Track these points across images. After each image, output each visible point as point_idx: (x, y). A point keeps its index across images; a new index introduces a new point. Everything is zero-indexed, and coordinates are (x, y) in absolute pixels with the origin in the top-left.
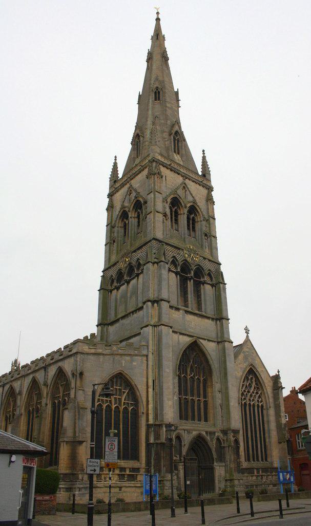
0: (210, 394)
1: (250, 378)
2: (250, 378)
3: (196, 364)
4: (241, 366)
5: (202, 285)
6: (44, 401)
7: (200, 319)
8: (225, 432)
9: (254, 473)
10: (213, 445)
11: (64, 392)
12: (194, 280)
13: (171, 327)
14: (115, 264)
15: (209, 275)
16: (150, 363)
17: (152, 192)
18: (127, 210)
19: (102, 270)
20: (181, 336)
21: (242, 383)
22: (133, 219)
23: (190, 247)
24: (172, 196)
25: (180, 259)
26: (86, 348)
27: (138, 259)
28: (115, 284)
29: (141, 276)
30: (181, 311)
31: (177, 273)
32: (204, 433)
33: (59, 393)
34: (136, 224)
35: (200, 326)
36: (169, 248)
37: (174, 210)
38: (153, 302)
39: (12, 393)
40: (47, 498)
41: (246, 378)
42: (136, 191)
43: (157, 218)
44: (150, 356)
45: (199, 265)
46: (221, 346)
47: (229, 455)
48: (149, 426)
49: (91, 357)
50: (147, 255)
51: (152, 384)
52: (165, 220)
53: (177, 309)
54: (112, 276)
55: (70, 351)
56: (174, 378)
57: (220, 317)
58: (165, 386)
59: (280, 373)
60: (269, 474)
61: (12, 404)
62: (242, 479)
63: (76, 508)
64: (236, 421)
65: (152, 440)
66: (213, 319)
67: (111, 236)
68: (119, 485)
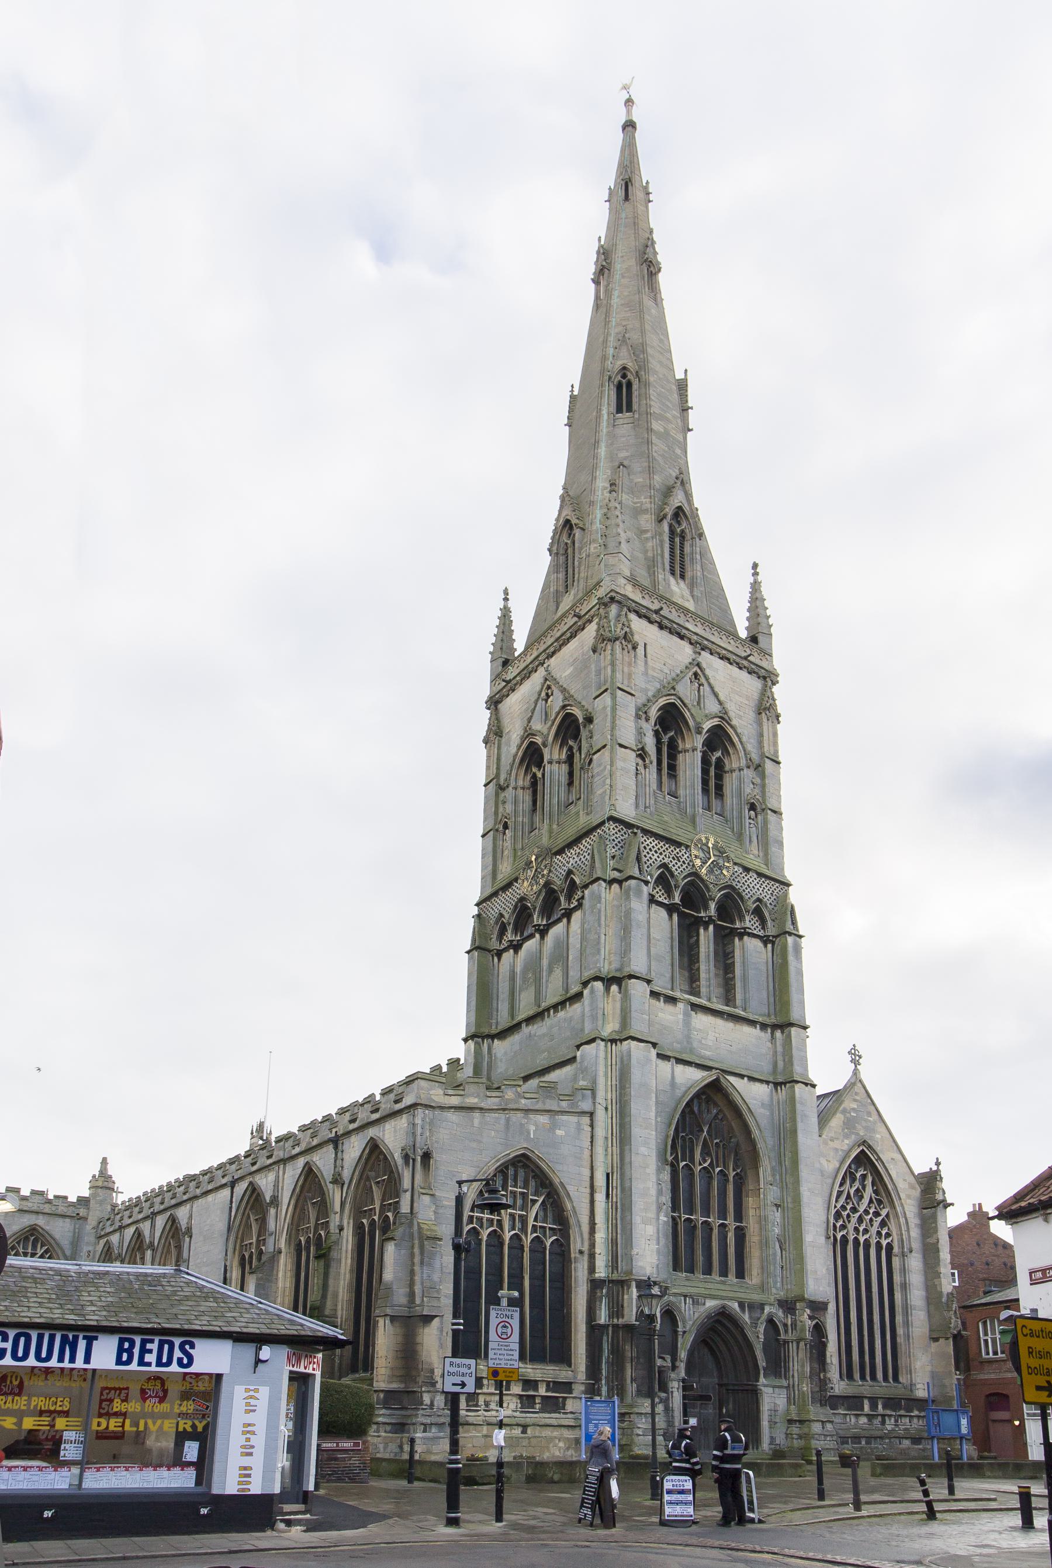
0: (751, 1212)
1: (858, 1175)
2: (858, 1175)
3: (715, 1141)
4: (836, 1144)
5: (737, 940)
6: (335, 1221)
7: (730, 1025)
8: (788, 1306)
9: (862, 1409)
10: (758, 1336)
11: (383, 1200)
12: (716, 926)
13: (654, 1045)
14: (508, 886)
15: (758, 912)
16: (600, 1132)
17: (606, 690)
18: (539, 740)
19: (476, 900)
20: (680, 1068)
21: (836, 1188)
22: (555, 767)
23: (707, 839)
25: (679, 870)
26: (437, 1095)
27: (570, 872)
28: (509, 936)
29: (577, 916)
30: (681, 1005)
31: (670, 909)
32: (736, 1305)
33: (373, 1202)
34: (564, 779)
35: (722, 1040)
36: (651, 842)
39: (255, 1203)
40: (347, 1444)
41: (850, 1175)
42: (563, 690)
43: (619, 764)
44: (600, 1114)
45: (731, 887)
46: (783, 1093)
47: (799, 1362)
48: (595, 1285)
49: (452, 1116)
50: (593, 857)
51: (605, 1184)
52: (641, 768)
53: (672, 1000)
54: (501, 915)
55: (396, 1102)
56: (659, 1171)
57: (783, 1022)
58: (637, 1187)
59: (941, 1167)
60: (902, 1412)
61: (255, 1228)
62: (832, 1422)
63: (418, 1472)
64: (819, 1278)
65: (603, 1317)
66: (764, 1026)
68: (522, 1421)
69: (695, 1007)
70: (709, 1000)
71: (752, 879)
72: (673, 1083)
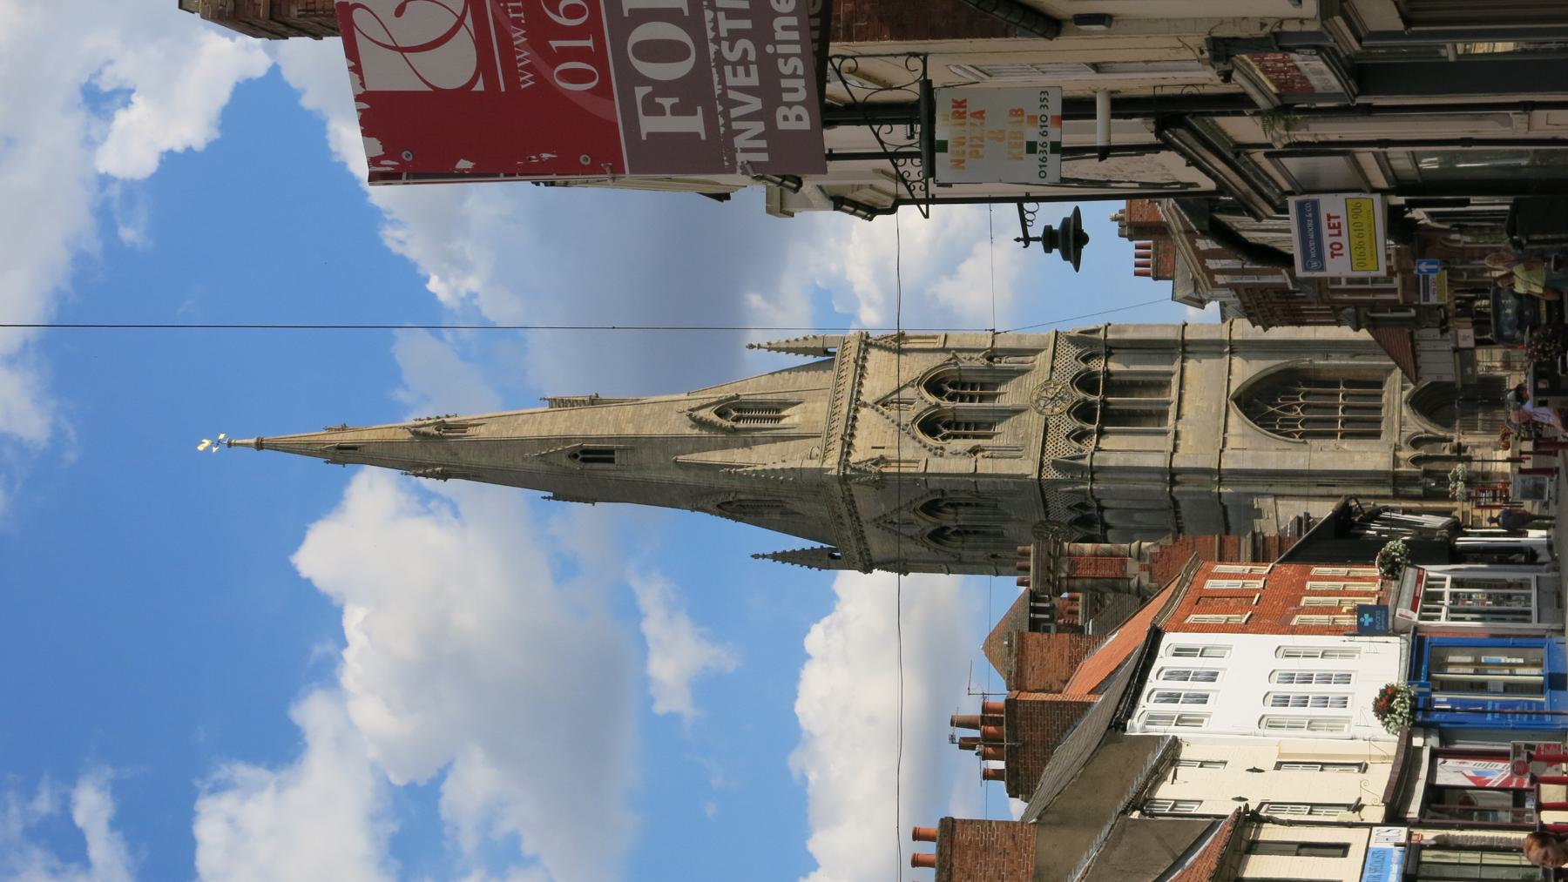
7: (1187, 387)
12: (1107, 392)
15: (1086, 360)
16: (1288, 490)
24: (920, 435)
29: (1104, 503)
36: (1049, 447)
37: (946, 432)
38: (1173, 482)
53: (1177, 435)
65: (1418, 491)
67: (981, 564)
69: (1178, 417)
70: (1169, 403)
71: (1058, 364)
72: (1243, 436)
